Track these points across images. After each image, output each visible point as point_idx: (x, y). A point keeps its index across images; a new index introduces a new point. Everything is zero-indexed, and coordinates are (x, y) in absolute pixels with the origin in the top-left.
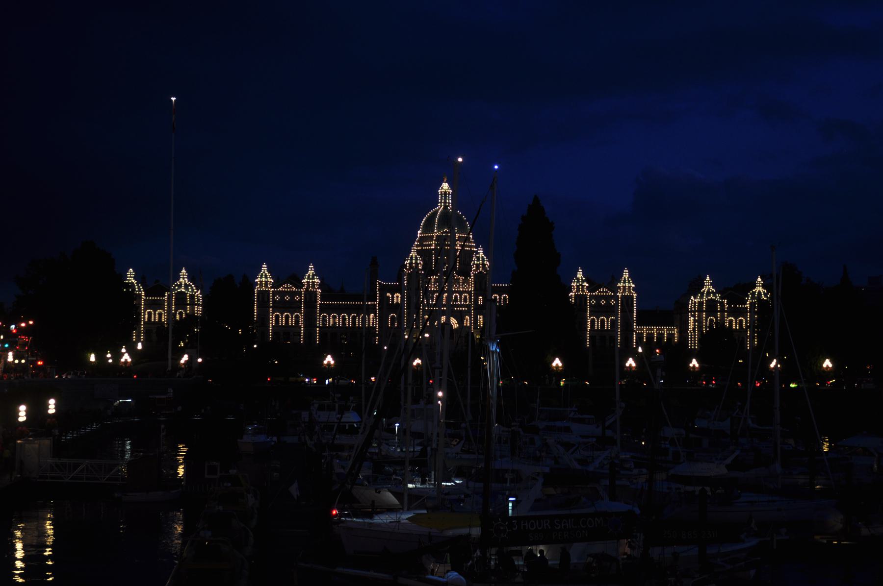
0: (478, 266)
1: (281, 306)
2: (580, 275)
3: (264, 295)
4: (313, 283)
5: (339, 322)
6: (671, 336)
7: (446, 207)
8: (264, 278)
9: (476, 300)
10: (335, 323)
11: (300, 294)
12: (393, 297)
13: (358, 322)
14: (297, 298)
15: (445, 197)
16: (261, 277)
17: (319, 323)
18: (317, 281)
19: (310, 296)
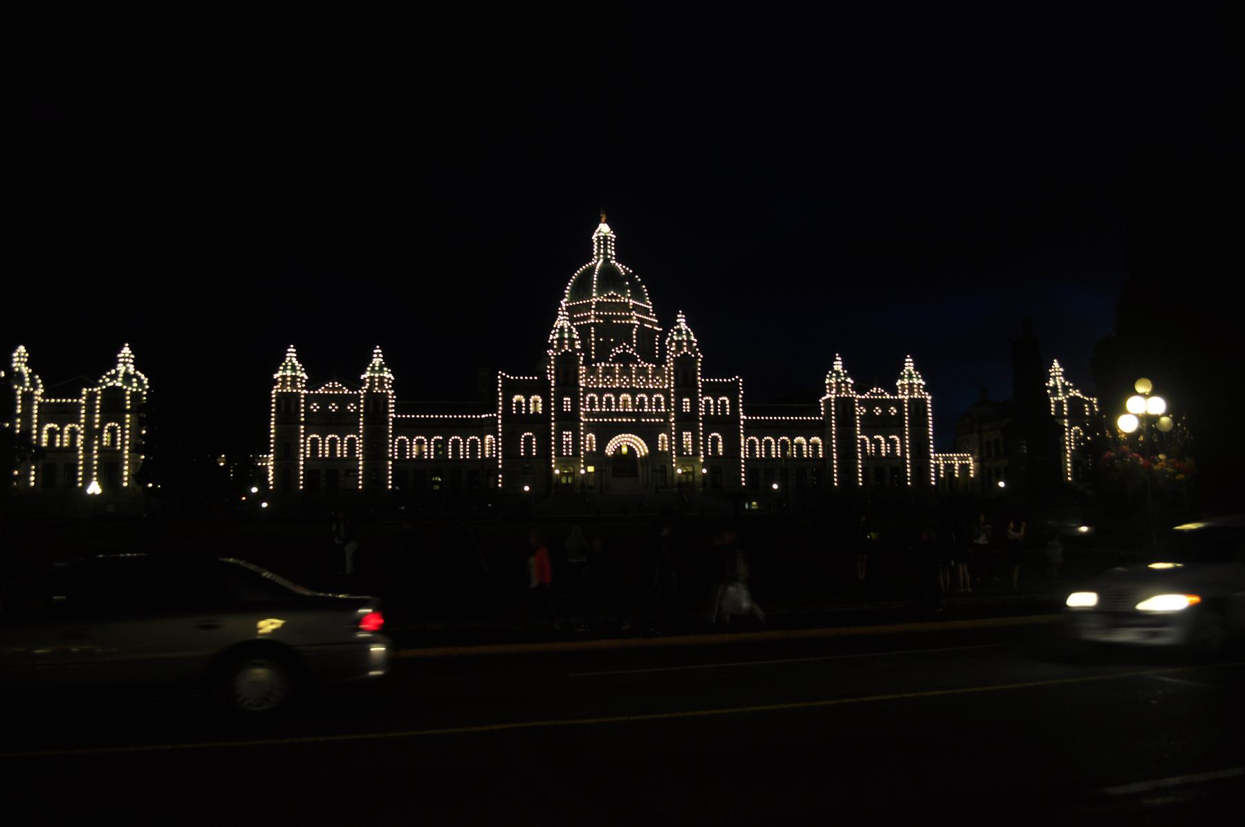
0: (679, 344)
1: (322, 423)
2: (838, 366)
3: (289, 401)
4: (381, 378)
5: (429, 451)
6: (964, 468)
7: (606, 261)
8: (291, 370)
9: (679, 404)
10: (421, 453)
11: (356, 399)
12: (528, 402)
13: (464, 452)
14: (351, 408)
15: (605, 244)
16: (285, 369)
17: (393, 451)
18: (387, 375)
19: (376, 403)
